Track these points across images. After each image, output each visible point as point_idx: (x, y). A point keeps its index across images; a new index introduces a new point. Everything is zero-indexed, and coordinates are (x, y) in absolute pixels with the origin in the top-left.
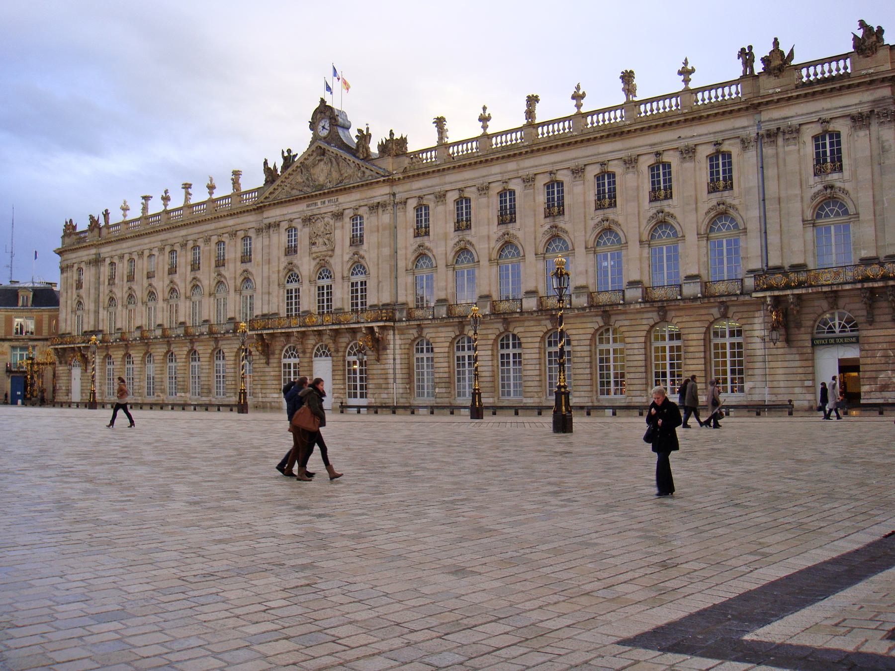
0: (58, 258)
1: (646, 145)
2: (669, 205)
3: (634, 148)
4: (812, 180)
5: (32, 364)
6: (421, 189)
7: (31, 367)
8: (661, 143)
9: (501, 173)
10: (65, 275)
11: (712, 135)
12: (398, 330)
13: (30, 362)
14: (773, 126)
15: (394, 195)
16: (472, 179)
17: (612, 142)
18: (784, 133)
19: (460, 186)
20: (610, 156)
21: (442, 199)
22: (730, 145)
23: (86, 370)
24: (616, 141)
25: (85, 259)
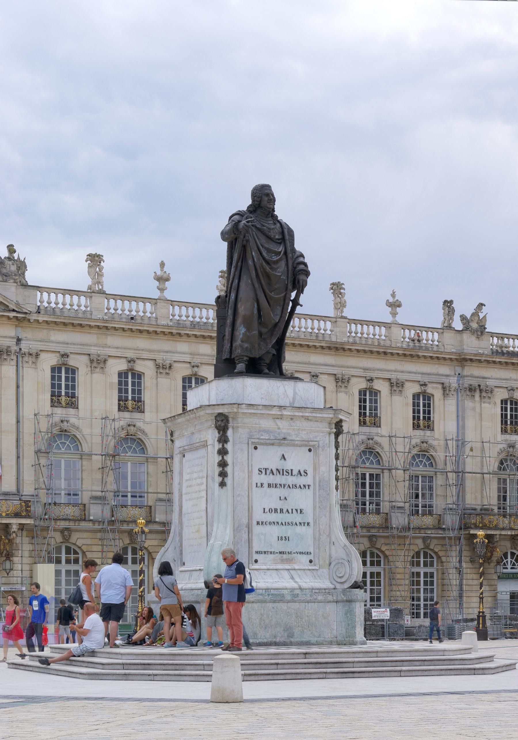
1: (360, 368)
2: (377, 434)
3: (348, 367)
4: (500, 437)
6: (67, 344)
8: (374, 370)
9: (191, 354)
11: (420, 375)
12: (27, 530)
14: (474, 382)
15: (19, 340)
16: (150, 351)
17: (347, 356)
18: (481, 391)
19: (130, 354)
20: (322, 369)
21: (102, 365)
22: (433, 388)
24: (317, 353)
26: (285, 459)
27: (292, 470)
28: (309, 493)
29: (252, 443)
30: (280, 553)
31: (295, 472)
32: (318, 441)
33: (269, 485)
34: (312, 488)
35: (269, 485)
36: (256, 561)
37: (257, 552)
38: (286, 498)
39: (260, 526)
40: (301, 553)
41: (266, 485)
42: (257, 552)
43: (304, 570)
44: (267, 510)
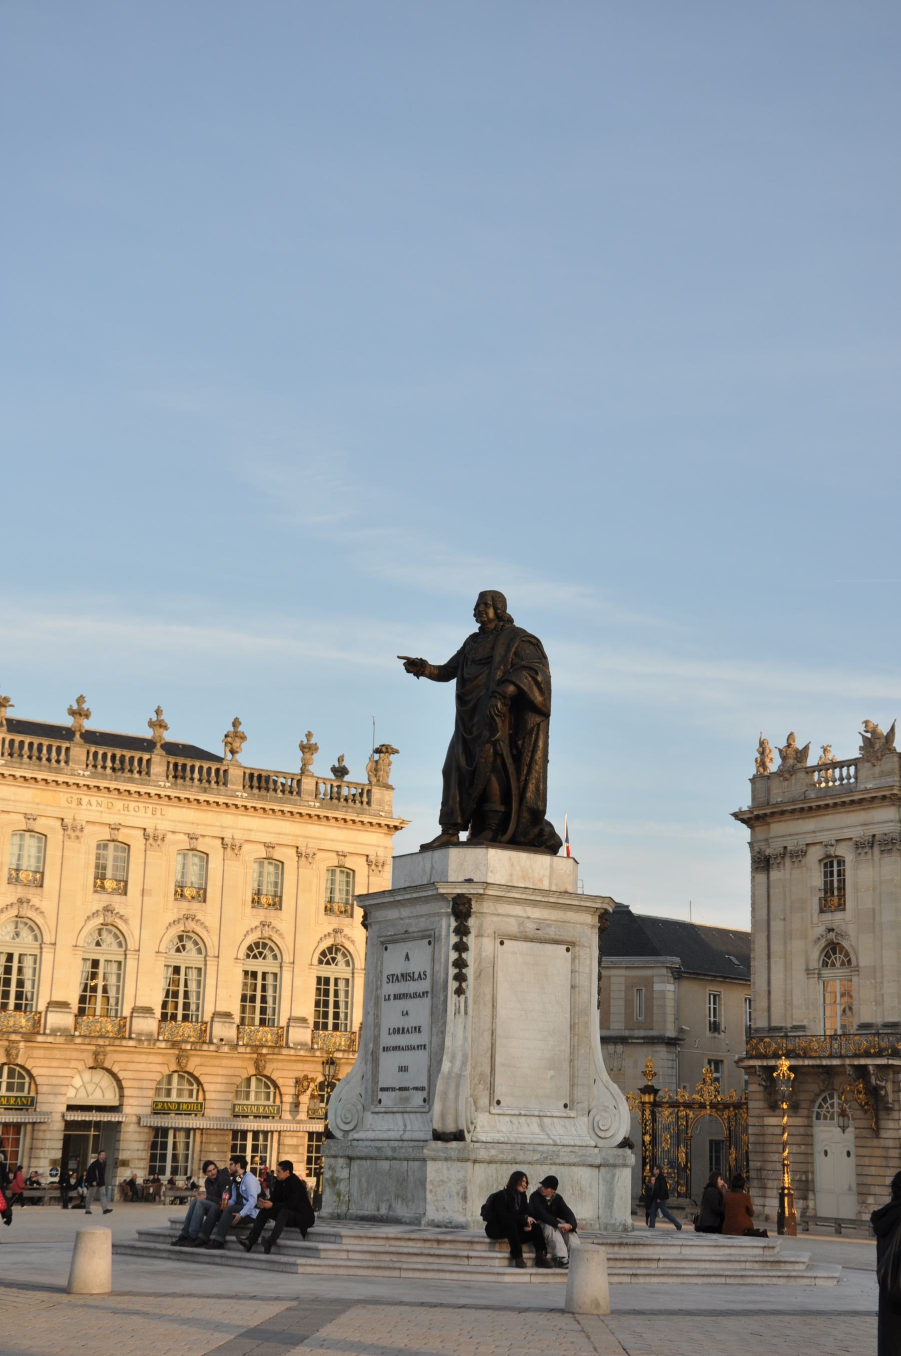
0: (745, 833)
5: (655, 1105)
7: (653, 1113)
10: (775, 875)
13: (647, 1098)
23: (876, 1132)
25: (856, 833)
26: (409, 960)
27: (414, 973)
28: (426, 1002)
29: (382, 943)
30: (401, 1089)
31: (416, 976)
32: (434, 929)
33: (395, 997)
34: (429, 995)
35: (395, 997)
36: (380, 1101)
37: (383, 1089)
38: (407, 1013)
39: (386, 1053)
40: (416, 1089)
41: (392, 997)
42: (383, 1089)
43: (416, 1112)
44: (391, 1031)
